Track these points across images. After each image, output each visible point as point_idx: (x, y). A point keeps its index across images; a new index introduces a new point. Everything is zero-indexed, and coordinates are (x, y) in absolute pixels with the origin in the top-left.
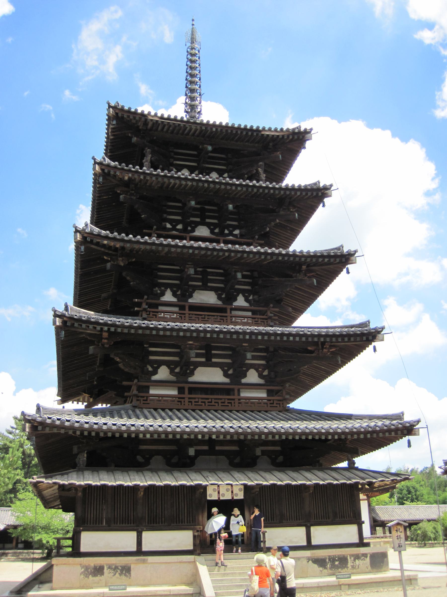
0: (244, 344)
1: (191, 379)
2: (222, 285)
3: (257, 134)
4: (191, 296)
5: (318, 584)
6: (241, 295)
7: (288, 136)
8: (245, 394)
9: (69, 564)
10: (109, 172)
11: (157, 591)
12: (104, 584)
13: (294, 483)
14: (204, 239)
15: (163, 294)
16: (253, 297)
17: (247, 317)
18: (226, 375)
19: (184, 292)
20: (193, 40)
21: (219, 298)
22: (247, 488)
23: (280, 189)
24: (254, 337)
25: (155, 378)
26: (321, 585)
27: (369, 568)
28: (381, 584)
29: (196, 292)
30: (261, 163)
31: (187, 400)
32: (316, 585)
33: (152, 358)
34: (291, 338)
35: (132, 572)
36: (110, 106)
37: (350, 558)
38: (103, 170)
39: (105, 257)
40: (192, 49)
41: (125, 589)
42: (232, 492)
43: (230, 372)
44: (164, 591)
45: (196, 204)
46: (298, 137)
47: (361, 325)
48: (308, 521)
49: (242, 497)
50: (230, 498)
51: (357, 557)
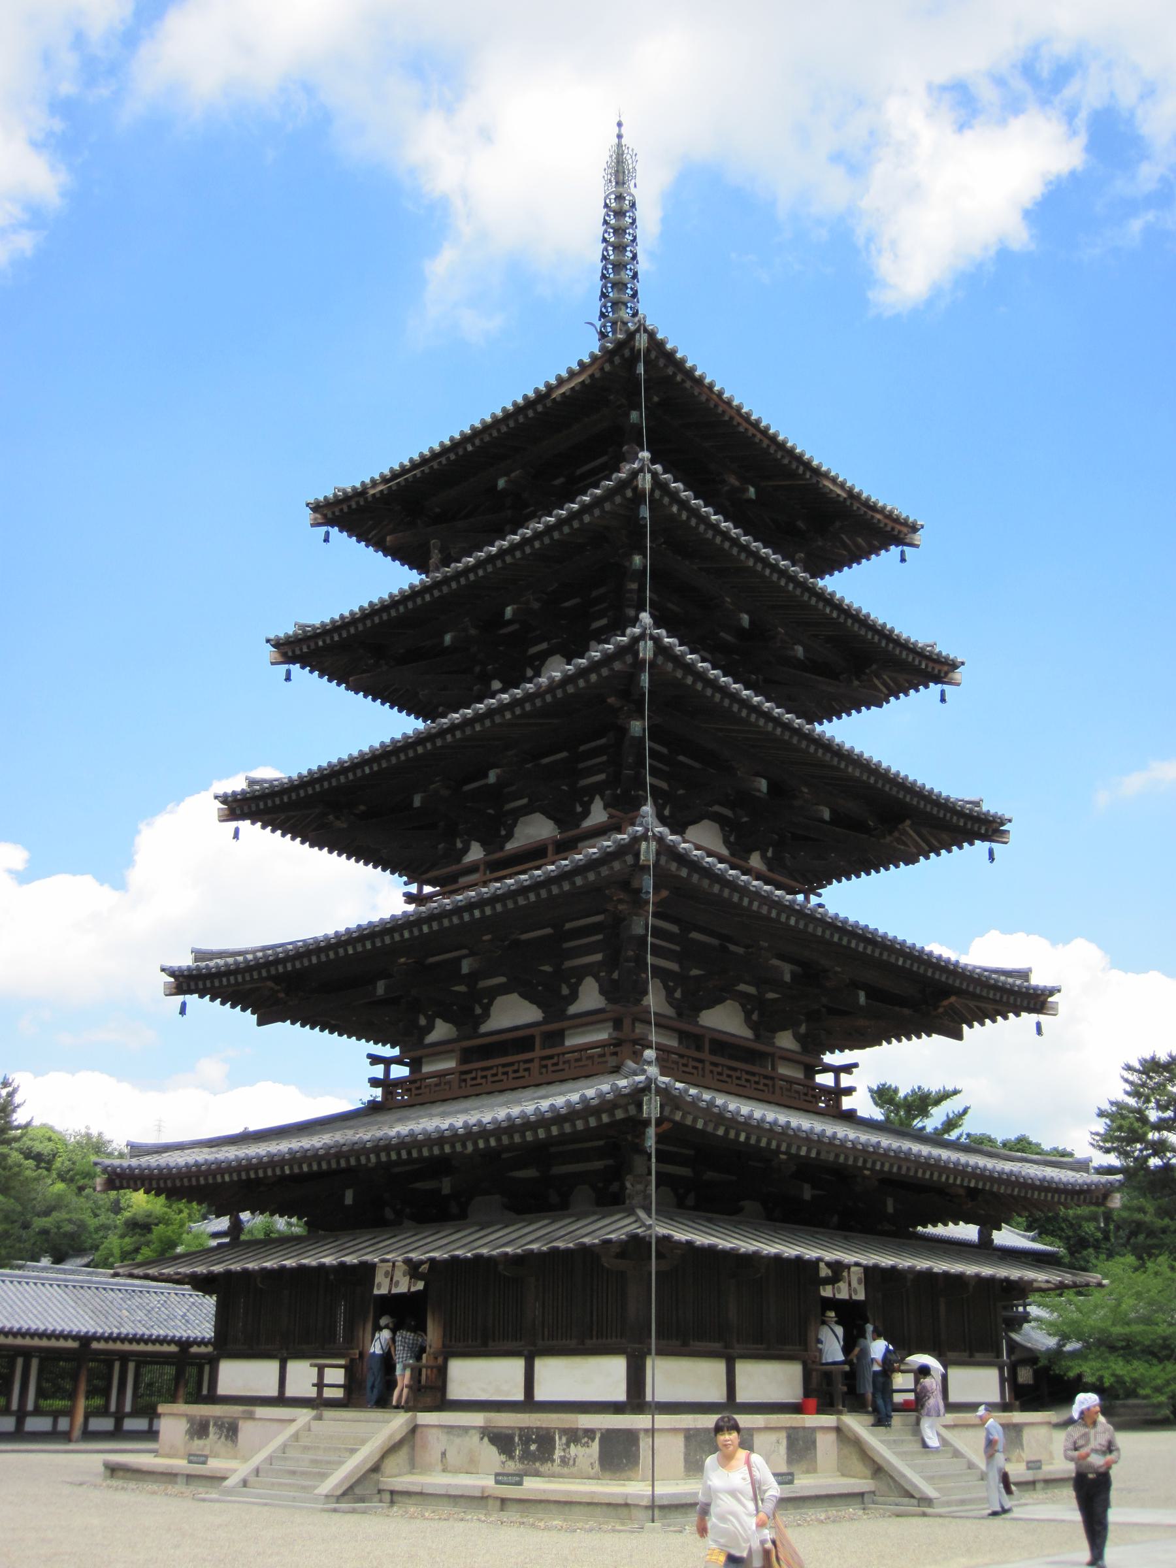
1: (484, 1028)
4: (510, 836)
5: (483, 1492)
6: (598, 798)
8: (574, 1040)
15: (466, 850)
19: (494, 832)
28: (567, 1508)
29: (519, 824)
30: (625, 448)
32: (443, 1492)
35: (241, 1435)
37: (560, 1438)
51: (574, 1436)
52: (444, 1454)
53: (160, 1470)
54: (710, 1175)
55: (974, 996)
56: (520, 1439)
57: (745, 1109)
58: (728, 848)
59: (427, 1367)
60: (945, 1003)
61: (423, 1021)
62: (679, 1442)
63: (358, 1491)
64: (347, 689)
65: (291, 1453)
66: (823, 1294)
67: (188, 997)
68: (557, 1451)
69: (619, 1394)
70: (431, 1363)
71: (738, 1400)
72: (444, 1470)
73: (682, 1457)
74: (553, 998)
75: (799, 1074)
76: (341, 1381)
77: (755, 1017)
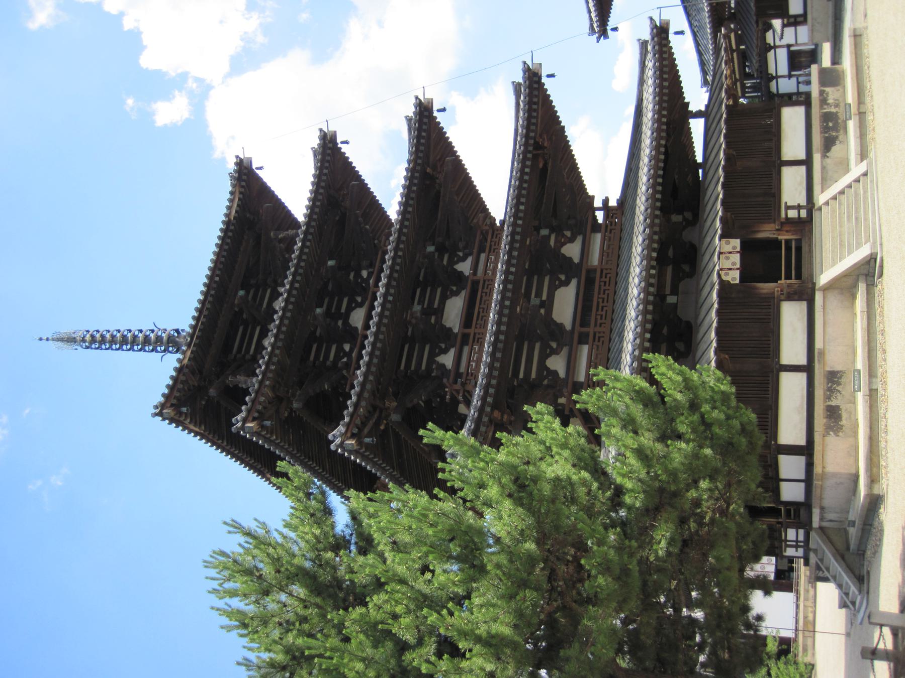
0: (528, 243)
1: (568, 327)
2: (439, 290)
3: (233, 224)
6: (456, 267)
7: (243, 187)
9: (823, 451)
10: (258, 412)
11: (862, 328)
12: (852, 405)
13: (716, 306)
14: (369, 317)
16: (460, 251)
17: (488, 259)
18: (566, 283)
19: (443, 338)
20: (70, 340)
21: (456, 294)
22: (724, 236)
23: (308, 224)
24: (521, 215)
25: (562, 374)
26: (858, 134)
27: (838, 88)
31: (598, 329)
32: (858, 140)
33: (533, 376)
34: (527, 170)
35: (838, 368)
36: (160, 414)
38: (254, 419)
39: (382, 427)
40: (83, 340)
41: (859, 371)
42: (730, 253)
43: (563, 277)
44: (862, 319)
45: (321, 306)
46: (245, 174)
47: (517, 93)
48: (774, 163)
49: (738, 241)
50: (738, 255)
51: (823, 101)
53: (868, 409)
69: (800, 110)
74: (566, 270)
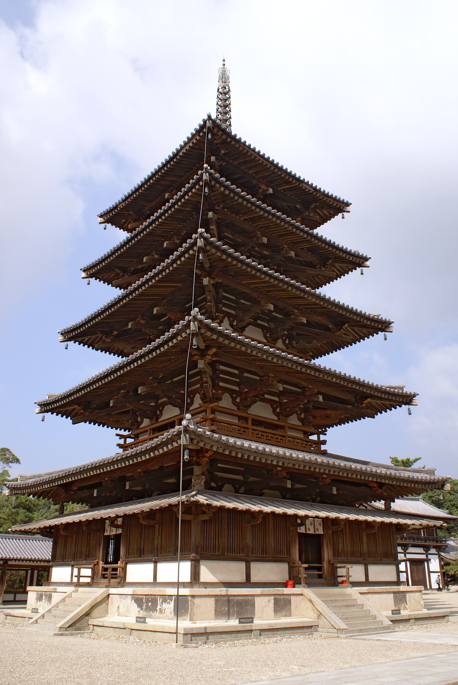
27: (173, 613)
35: (52, 599)
37: (160, 600)
52: (118, 607)
54: (252, 479)
55: (380, 398)
56: (145, 600)
57: (239, 442)
58: (266, 339)
59: (120, 567)
60: (365, 402)
61: (139, 419)
62: (212, 601)
63: (78, 625)
64: (112, 286)
65: (61, 607)
66: (299, 531)
67: (45, 414)
68: (158, 606)
70: (121, 566)
71: (252, 581)
72: (118, 615)
73: (213, 609)
75: (301, 436)
76: (90, 575)
77: (278, 410)
